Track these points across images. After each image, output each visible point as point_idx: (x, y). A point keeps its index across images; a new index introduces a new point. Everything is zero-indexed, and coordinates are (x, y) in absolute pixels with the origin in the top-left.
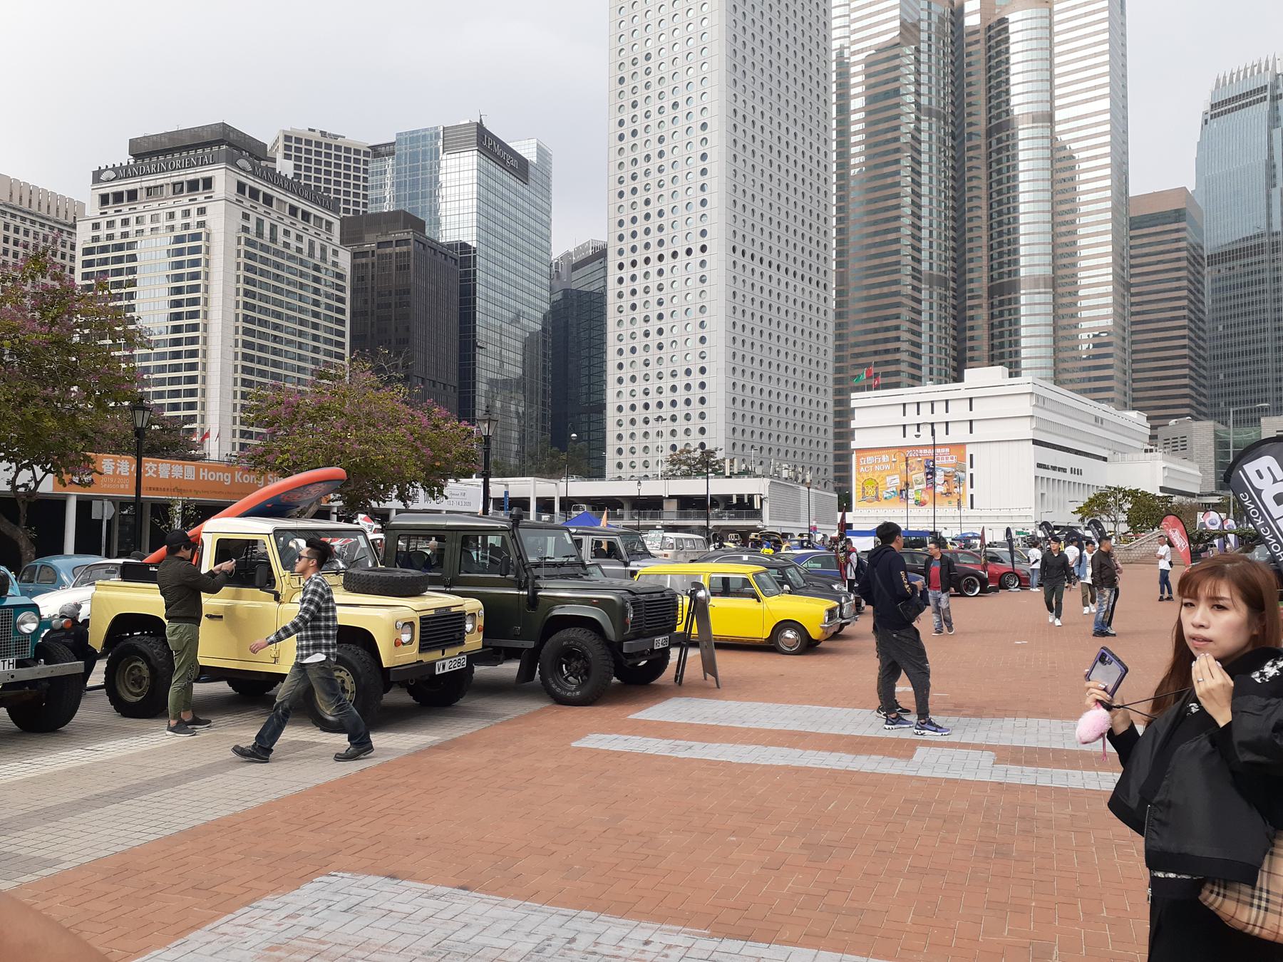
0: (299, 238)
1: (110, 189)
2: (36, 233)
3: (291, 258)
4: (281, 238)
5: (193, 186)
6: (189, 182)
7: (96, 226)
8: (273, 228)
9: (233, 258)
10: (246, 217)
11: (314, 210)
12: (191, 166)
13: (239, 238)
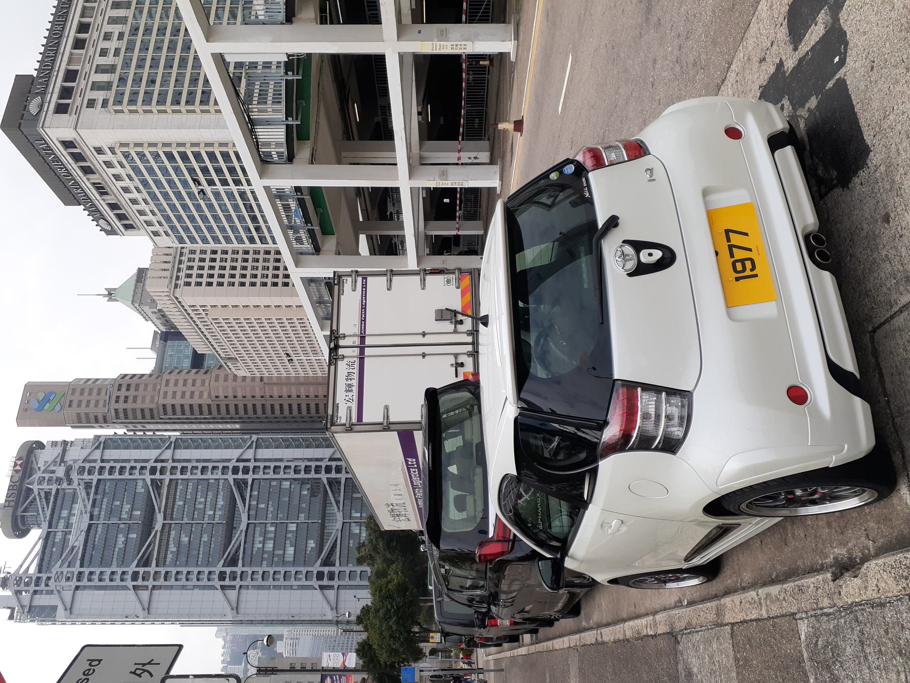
0: (107, 37)
1: (117, 224)
2: (189, 260)
4: (109, 60)
7: (156, 234)
8: (100, 69)
9: (139, 118)
10: (91, 103)
11: (75, 19)
12: (57, 159)
13: (116, 111)
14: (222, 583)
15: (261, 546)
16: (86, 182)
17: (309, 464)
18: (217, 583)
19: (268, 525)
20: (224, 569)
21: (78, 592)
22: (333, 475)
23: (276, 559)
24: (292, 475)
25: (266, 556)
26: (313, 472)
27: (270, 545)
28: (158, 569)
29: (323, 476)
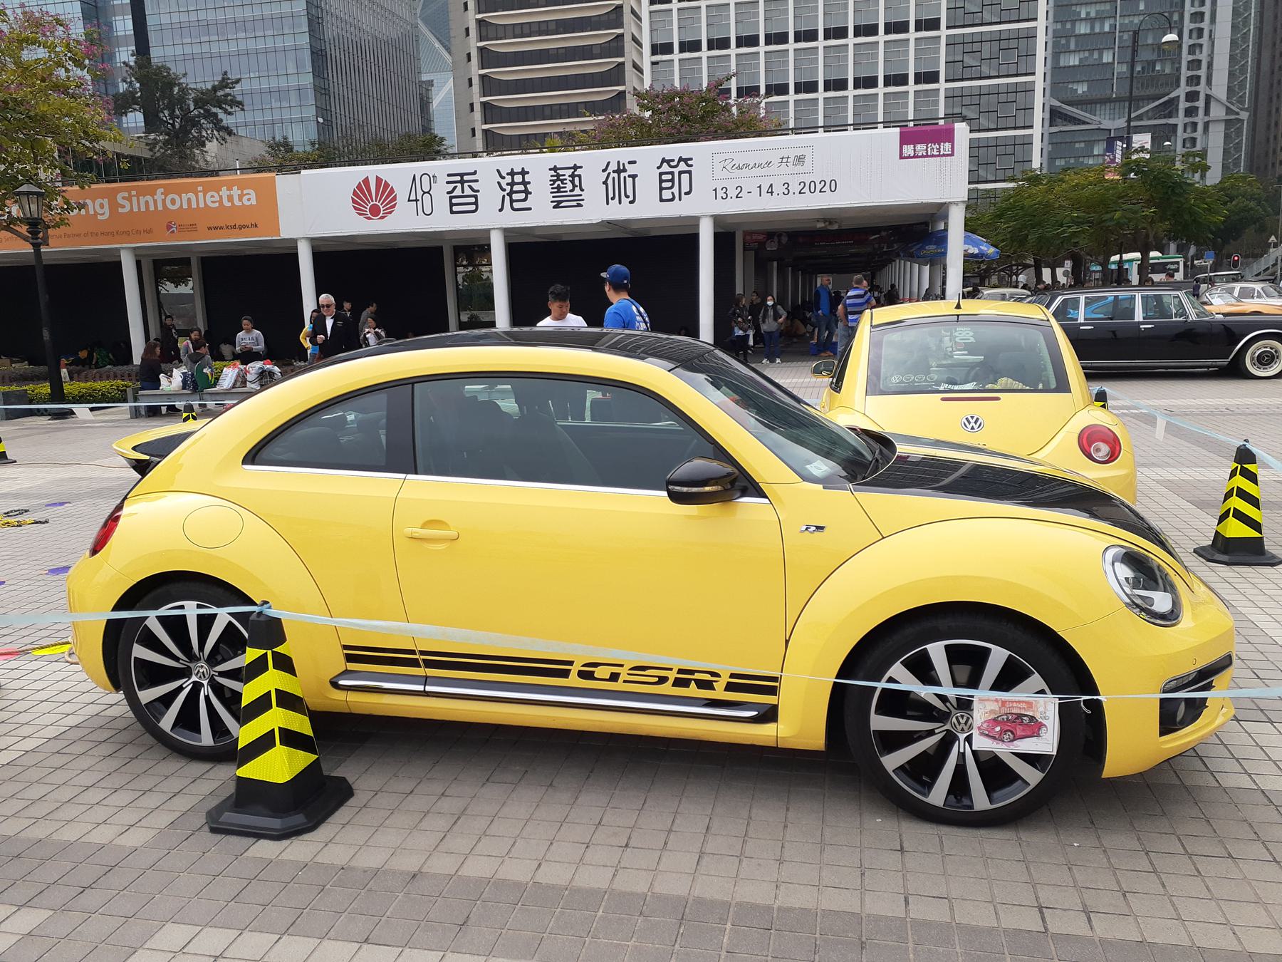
15: (1083, 16)
17: (1204, 65)
19: (1112, 21)
22: (1183, 105)
23: (1063, 41)
24: (1187, 42)
25: (1068, 26)
26: (1190, 73)
27: (1083, 29)
29: (1182, 91)
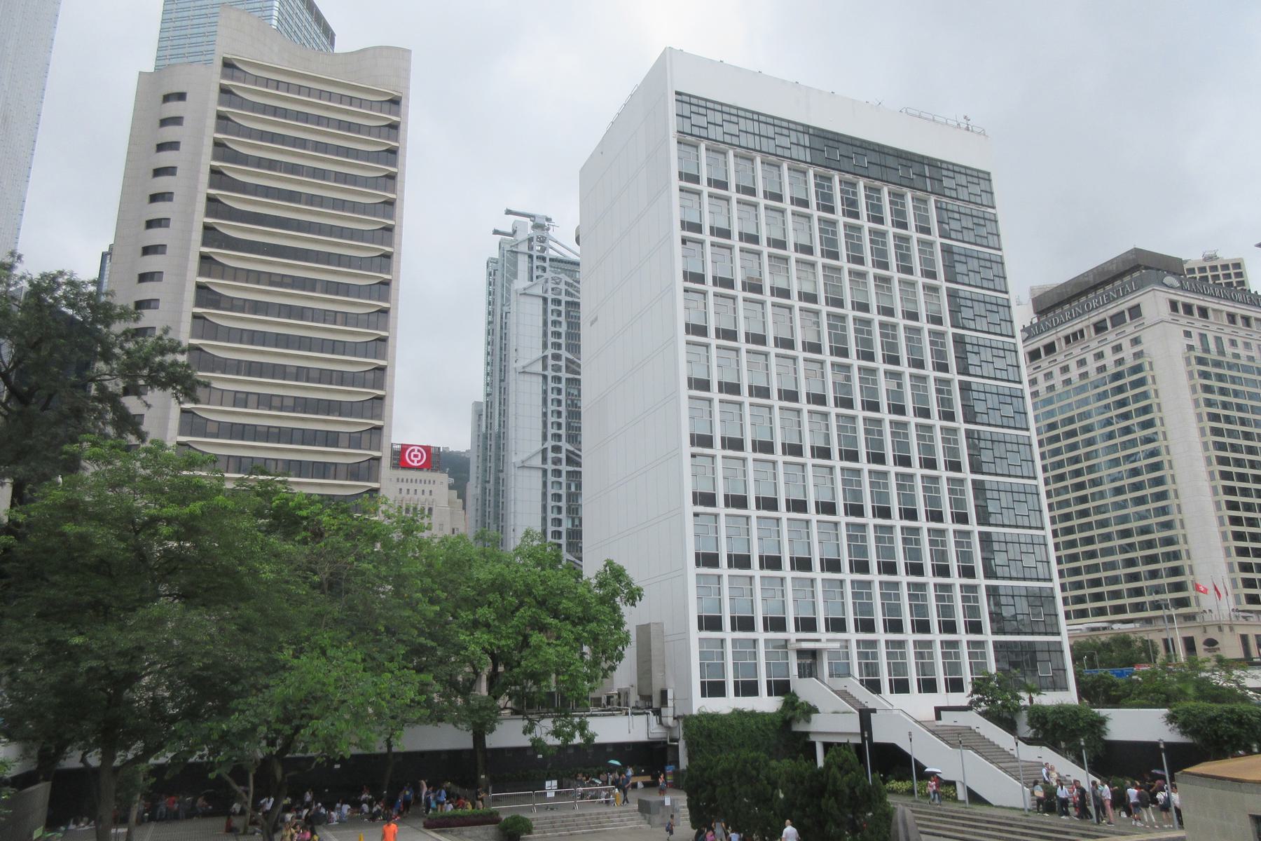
3: (1247, 369)
4: (1229, 350)
5: (1118, 319)
6: (1112, 318)
8: (1218, 340)
10: (1188, 334)
14: (550, 449)
16: (1085, 323)
18: (550, 443)
20: (564, 451)
21: (541, 301)
28: (564, 381)
